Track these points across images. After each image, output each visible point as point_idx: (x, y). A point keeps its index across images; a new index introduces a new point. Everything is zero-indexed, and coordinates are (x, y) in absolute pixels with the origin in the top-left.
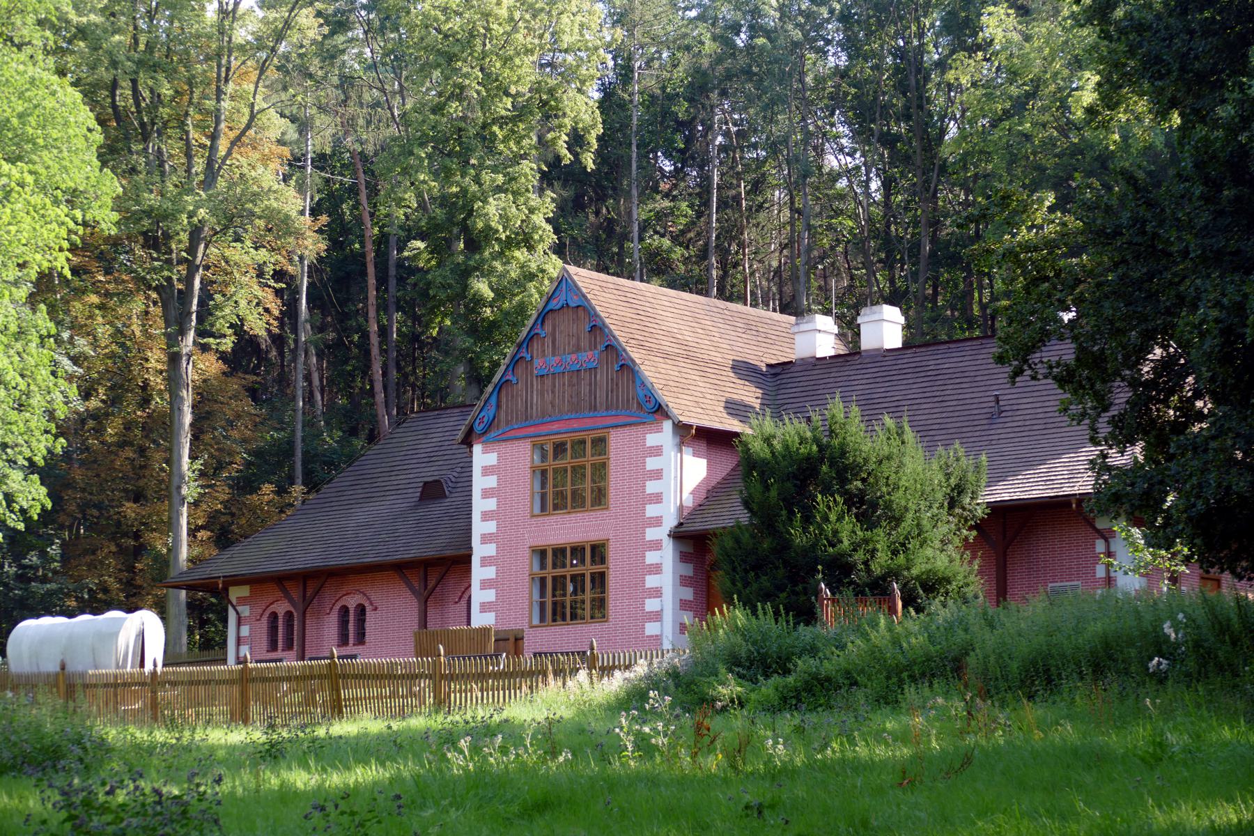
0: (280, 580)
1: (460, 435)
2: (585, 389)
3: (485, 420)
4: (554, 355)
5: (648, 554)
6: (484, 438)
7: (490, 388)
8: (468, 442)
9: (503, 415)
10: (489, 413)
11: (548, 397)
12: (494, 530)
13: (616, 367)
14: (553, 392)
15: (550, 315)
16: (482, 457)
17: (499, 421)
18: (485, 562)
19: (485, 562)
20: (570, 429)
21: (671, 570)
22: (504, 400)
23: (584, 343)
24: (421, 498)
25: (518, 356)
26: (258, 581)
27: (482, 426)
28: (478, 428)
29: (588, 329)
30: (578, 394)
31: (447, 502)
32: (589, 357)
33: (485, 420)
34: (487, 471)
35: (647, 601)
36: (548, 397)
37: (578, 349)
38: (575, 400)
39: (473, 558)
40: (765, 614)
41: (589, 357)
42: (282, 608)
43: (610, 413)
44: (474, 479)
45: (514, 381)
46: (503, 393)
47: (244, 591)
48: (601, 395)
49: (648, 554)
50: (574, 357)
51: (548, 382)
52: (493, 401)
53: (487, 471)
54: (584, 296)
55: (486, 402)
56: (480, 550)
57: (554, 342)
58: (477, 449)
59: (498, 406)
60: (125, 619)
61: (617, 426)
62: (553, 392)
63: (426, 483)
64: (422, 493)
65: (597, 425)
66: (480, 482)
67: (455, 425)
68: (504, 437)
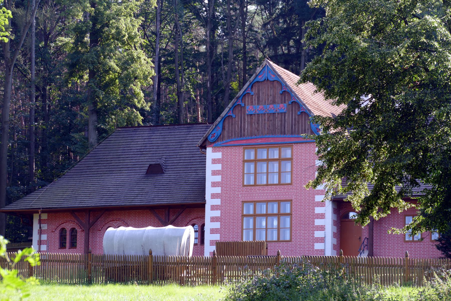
0: (75, 212)
1: (200, 142)
2: (278, 123)
3: (216, 135)
4: (258, 104)
5: (316, 208)
6: (214, 145)
7: (219, 119)
8: (203, 147)
9: (226, 133)
10: (218, 131)
11: (255, 126)
12: (220, 192)
13: (299, 113)
14: (258, 123)
15: (257, 84)
16: (211, 154)
17: (223, 137)
18: (213, 208)
19: (213, 208)
20: (269, 143)
21: (331, 217)
22: (227, 126)
23: (278, 99)
24: (147, 173)
25: (237, 104)
26: (53, 213)
27: (213, 138)
28: (211, 139)
29: (281, 92)
30: (274, 125)
31: (165, 176)
32: (282, 107)
33: (216, 135)
34: (215, 161)
35: (316, 232)
36: (255, 126)
37: (274, 102)
38: (271, 128)
39: (206, 205)
40: (189, 238)
41: (282, 107)
42: (68, 227)
43: (294, 136)
44: (207, 166)
45: (234, 116)
46: (226, 122)
47: (45, 216)
48: (288, 127)
49: (316, 208)
50: (271, 106)
51: (255, 118)
52: (221, 126)
53: (215, 161)
54: (279, 76)
55: (216, 126)
56: (210, 202)
57: (258, 98)
58: (209, 150)
59: (223, 128)
60: (184, 230)
61: (297, 143)
62: (258, 123)
63: (150, 165)
64: (148, 170)
65: (286, 142)
66: (210, 167)
67: (197, 136)
68: (224, 145)
